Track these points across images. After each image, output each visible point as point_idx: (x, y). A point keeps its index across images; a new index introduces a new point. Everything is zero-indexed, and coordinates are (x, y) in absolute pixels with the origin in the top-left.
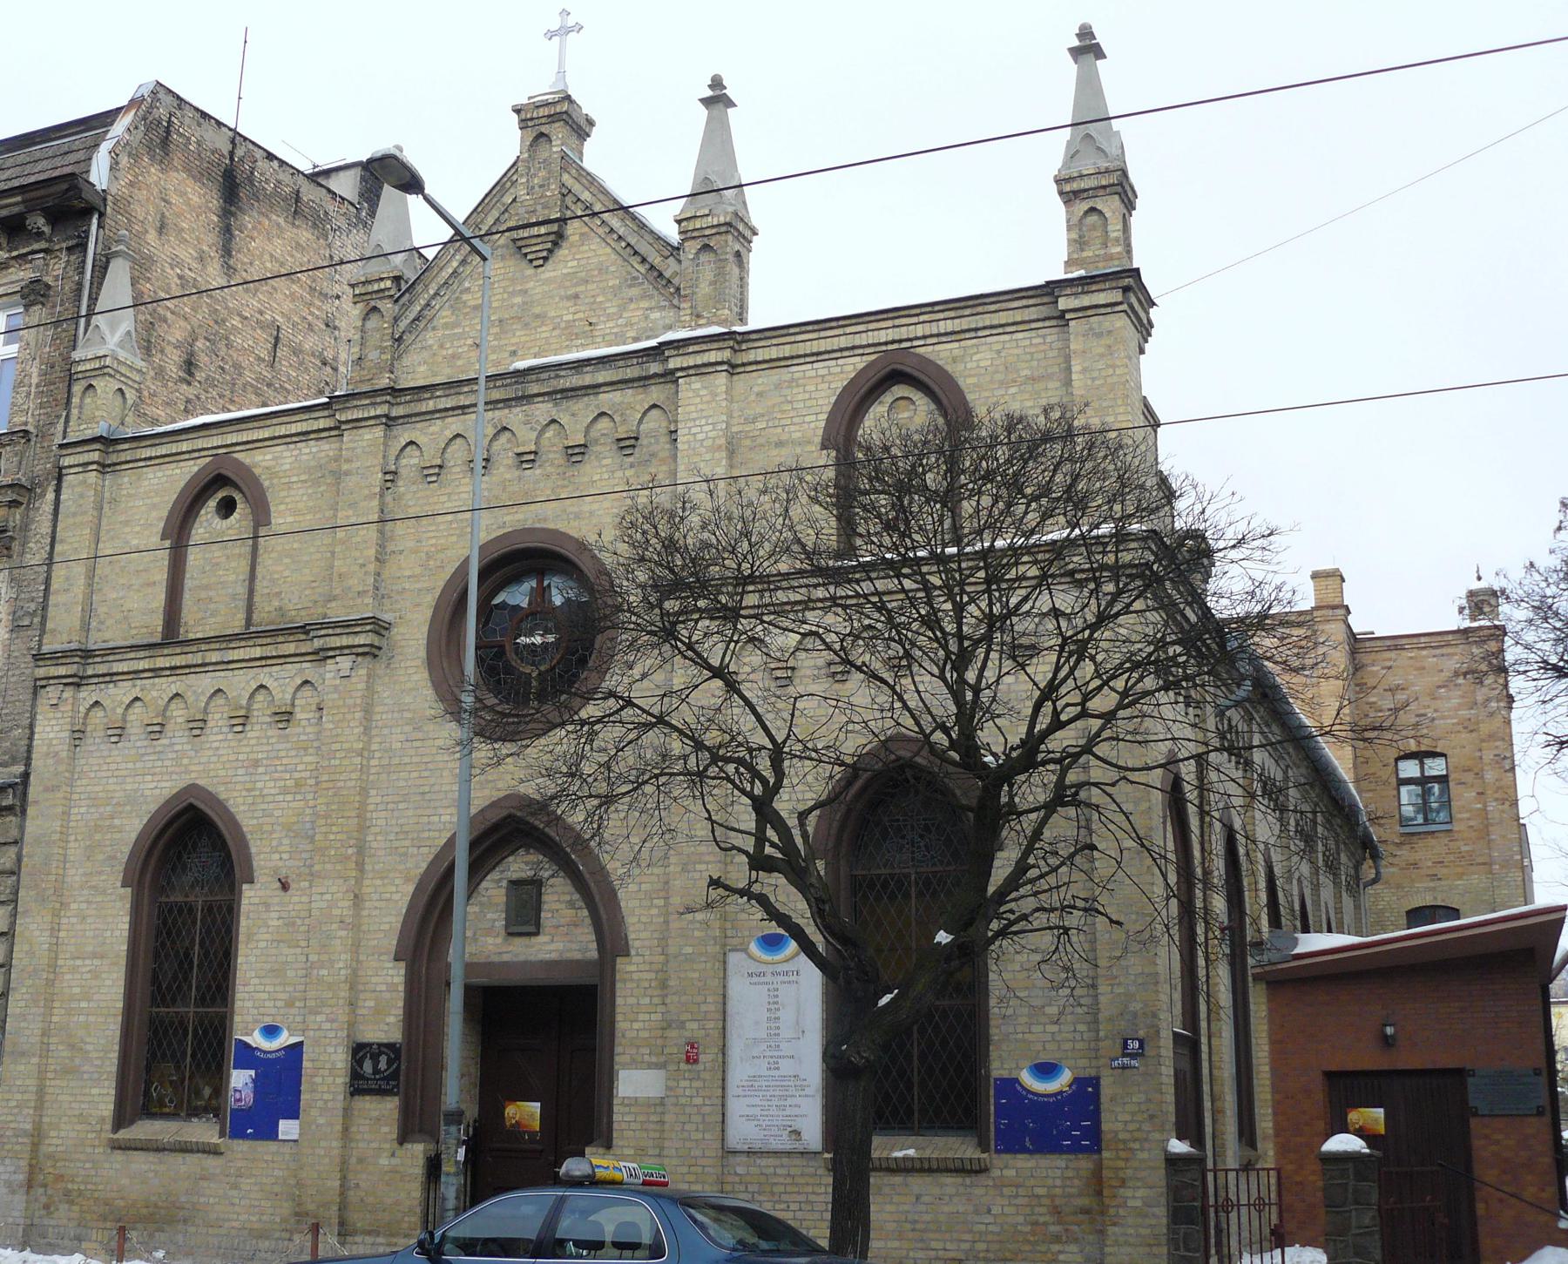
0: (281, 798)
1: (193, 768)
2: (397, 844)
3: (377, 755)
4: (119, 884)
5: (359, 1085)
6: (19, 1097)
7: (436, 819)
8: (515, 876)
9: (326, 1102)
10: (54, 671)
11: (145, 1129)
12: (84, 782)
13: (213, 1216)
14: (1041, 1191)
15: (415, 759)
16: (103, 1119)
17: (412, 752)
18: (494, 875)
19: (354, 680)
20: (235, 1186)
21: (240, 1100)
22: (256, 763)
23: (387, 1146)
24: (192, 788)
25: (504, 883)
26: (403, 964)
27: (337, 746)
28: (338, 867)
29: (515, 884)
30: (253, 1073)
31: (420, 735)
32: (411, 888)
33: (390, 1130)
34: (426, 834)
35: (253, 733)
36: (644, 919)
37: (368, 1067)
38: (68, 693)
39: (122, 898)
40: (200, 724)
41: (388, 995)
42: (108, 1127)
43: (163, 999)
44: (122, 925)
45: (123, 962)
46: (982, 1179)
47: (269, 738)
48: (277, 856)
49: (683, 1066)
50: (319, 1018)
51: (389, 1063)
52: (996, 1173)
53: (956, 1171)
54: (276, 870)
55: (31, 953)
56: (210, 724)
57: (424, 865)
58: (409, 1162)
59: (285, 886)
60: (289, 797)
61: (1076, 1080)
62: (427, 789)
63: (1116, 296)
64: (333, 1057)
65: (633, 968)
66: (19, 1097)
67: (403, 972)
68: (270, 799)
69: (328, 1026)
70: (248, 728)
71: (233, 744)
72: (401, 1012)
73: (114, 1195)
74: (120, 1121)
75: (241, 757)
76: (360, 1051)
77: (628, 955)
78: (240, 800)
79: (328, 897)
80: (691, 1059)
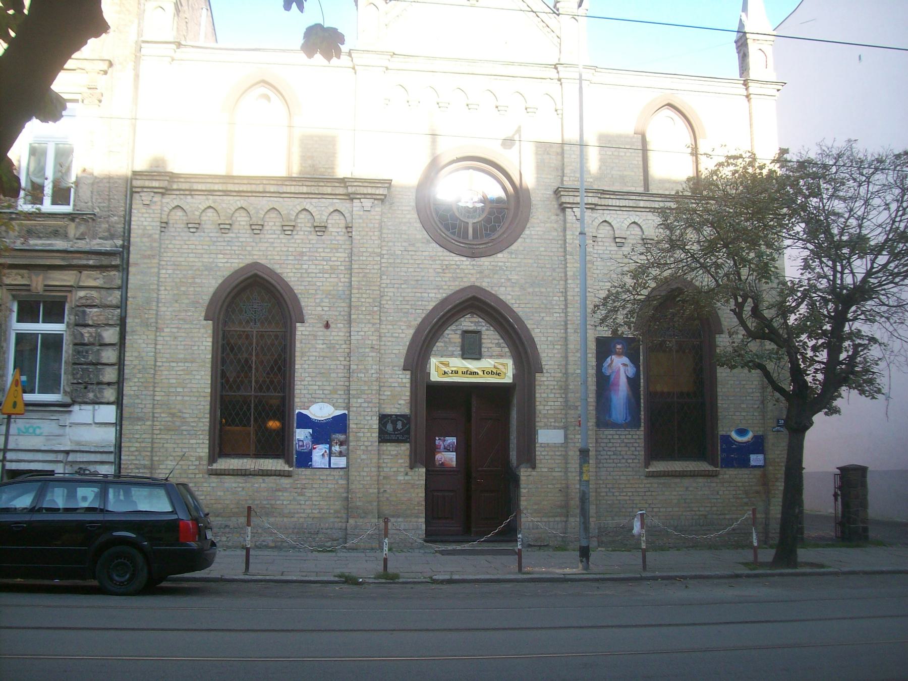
0: (321, 275)
1: (255, 253)
2: (400, 307)
3: (385, 256)
4: (202, 318)
5: (384, 437)
6: (138, 445)
7: (426, 295)
8: (465, 328)
9: (367, 446)
10: (147, 183)
11: (223, 464)
12: (169, 254)
13: (286, 511)
14: (740, 484)
15: (411, 261)
16: (200, 458)
17: (409, 257)
18: (453, 327)
19: (373, 213)
20: (302, 494)
21: (303, 446)
22: (302, 254)
23: (402, 470)
24: (256, 265)
25: (459, 332)
26: (409, 372)
27: (364, 250)
28: (368, 317)
29: (465, 332)
30: (311, 431)
31: (413, 249)
32: (412, 331)
33: (404, 461)
34: (420, 303)
35: (299, 236)
36: (550, 355)
37: (390, 427)
38: (157, 198)
39: (204, 327)
40: (260, 227)
41: (399, 389)
42: (205, 462)
43: (231, 388)
44: (208, 343)
45: (209, 365)
46: (715, 479)
47: (310, 240)
48: (320, 308)
49: (577, 428)
50: (359, 401)
51: (404, 425)
52: (721, 477)
53: (241, 475)
54: (320, 317)
55: (140, 358)
56: (266, 228)
57: (420, 320)
58: (416, 478)
59: (327, 326)
60: (326, 275)
61: (755, 437)
62: (420, 278)
63: (775, 92)
64: (370, 422)
65: (545, 379)
66: (138, 445)
67: (409, 376)
68: (314, 275)
69: (366, 405)
70: (295, 233)
71: (283, 241)
72: (408, 398)
73: (213, 502)
74: (212, 459)
75: (290, 249)
76: (384, 419)
77: (542, 372)
78: (291, 274)
79: (362, 333)
80: (580, 425)
